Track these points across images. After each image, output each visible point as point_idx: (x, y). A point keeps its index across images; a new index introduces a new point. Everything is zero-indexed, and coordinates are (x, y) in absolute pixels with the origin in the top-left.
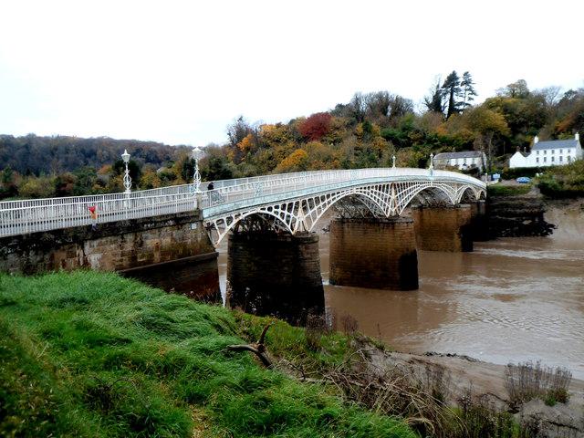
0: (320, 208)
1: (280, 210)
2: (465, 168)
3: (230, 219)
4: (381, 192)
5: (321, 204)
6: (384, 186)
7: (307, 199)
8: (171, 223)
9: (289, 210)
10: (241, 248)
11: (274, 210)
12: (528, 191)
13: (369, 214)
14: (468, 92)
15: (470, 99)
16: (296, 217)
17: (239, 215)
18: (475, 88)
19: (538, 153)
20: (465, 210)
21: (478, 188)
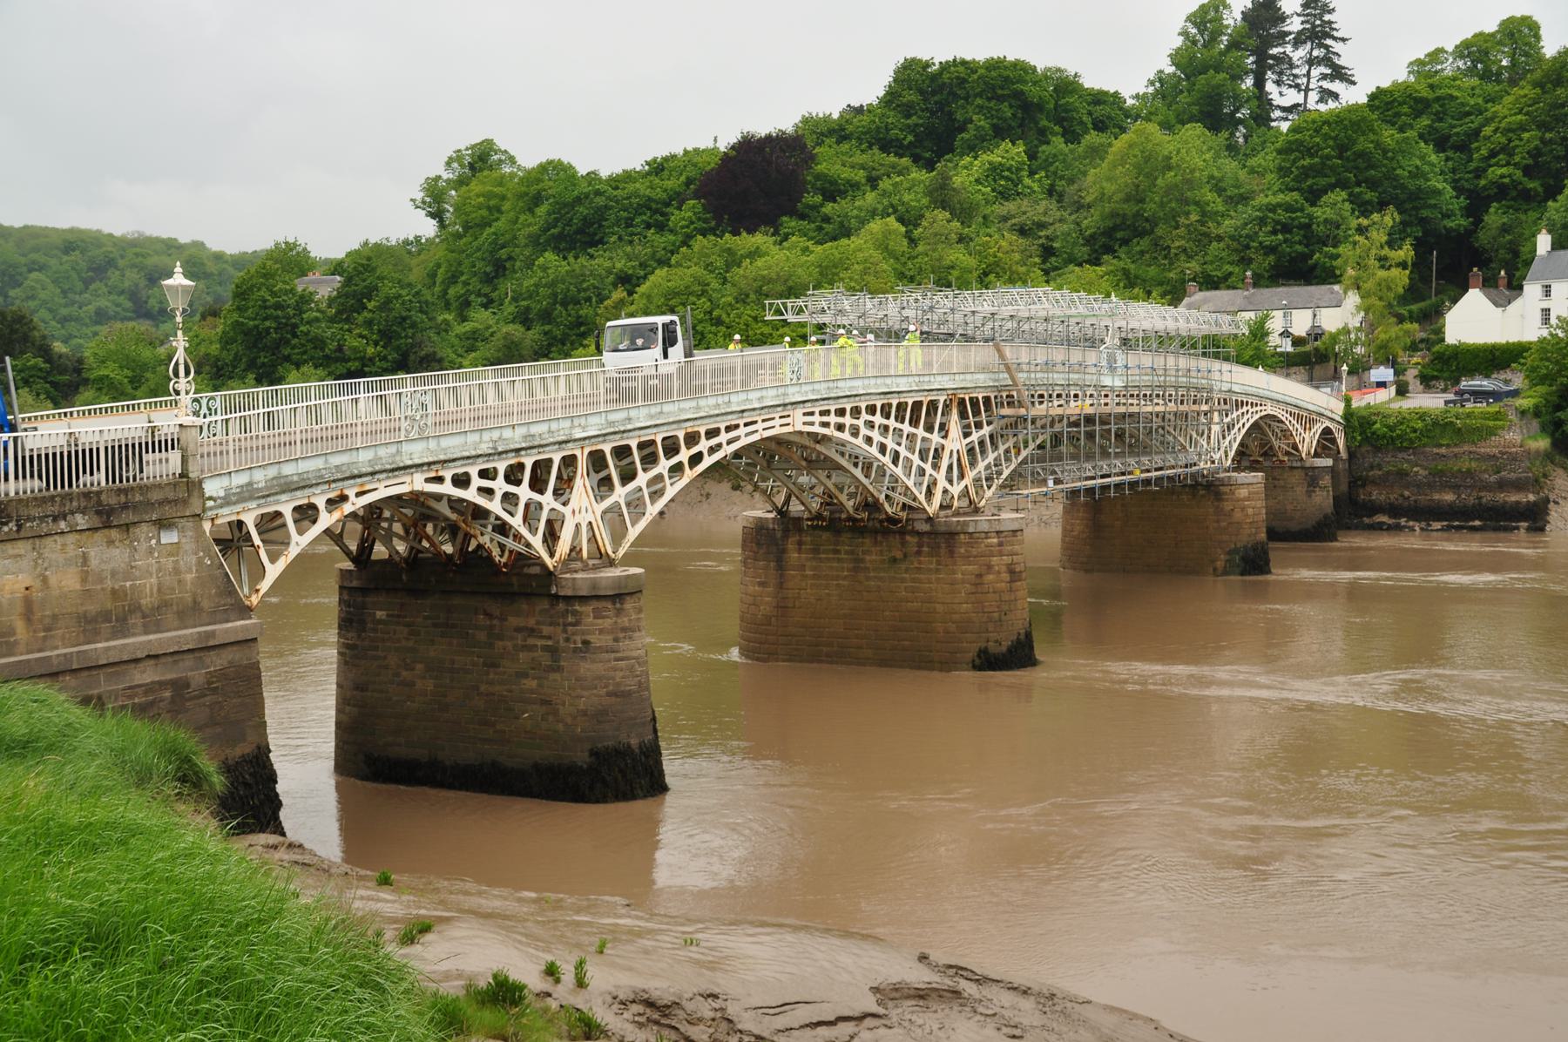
0: (659, 478)
1: (500, 486)
2: (1287, 347)
3: (306, 514)
4: (906, 428)
5: (664, 465)
6: (917, 405)
7: (607, 448)
8: (81, 521)
9: (538, 485)
10: (380, 614)
11: (477, 482)
12: (1492, 432)
13: (872, 506)
14: (1316, 72)
15: (1327, 95)
16: (566, 511)
17: (343, 498)
18: (1346, 56)
19: (1547, 291)
20: (1243, 492)
21: (1307, 418)
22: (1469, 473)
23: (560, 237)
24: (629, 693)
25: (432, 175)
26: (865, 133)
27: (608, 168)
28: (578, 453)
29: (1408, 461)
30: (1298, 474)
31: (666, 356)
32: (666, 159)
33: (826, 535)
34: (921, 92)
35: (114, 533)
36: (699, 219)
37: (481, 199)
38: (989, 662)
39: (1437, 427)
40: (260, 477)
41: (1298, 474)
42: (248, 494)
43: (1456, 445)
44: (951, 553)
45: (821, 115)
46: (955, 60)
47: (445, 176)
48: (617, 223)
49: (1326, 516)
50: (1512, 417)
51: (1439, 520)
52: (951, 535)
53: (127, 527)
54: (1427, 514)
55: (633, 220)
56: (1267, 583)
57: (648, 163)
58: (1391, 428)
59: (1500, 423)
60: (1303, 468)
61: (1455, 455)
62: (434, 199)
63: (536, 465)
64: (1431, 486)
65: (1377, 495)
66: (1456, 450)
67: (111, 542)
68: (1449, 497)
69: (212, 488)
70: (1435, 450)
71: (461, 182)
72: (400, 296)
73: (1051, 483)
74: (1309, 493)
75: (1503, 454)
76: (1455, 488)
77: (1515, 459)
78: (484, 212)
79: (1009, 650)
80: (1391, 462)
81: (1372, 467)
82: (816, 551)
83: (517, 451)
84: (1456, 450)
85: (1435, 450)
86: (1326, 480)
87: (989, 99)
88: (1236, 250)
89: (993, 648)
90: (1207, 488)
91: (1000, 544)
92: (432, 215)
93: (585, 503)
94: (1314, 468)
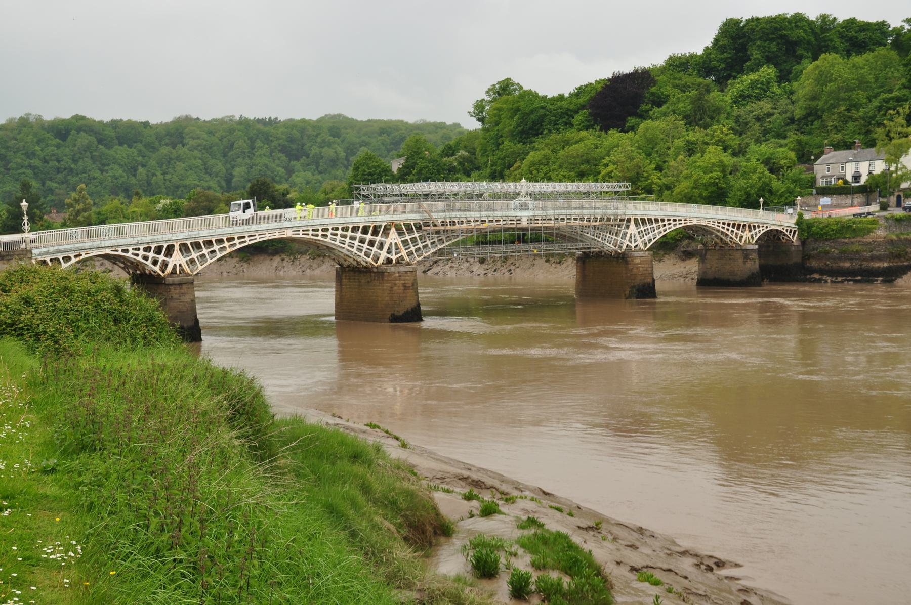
7: (188, 243)
11: (131, 251)
12: (870, 231)
20: (638, 261)
22: (857, 252)
23: (522, 132)
24: (183, 312)
25: (480, 99)
26: (696, 65)
27: (551, 93)
28: (175, 244)
29: (830, 246)
30: (740, 253)
31: (244, 212)
32: (586, 86)
33: (352, 273)
34: (732, 38)
35: (5, 261)
36: (586, 120)
37: (495, 112)
38: (395, 319)
39: (845, 228)
40: (51, 249)
41: (740, 253)
42: (47, 253)
43: (854, 238)
44: (383, 280)
45: (680, 55)
46: (752, 18)
47: (487, 98)
48: (550, 123)
49: (753, 274)
50: (882, 222)
51: (842, 276)
52: (383, 273)
53: (9, 260)
54: (837, 273)
55: (558, 121)
56: (655, 303)
57: (576, 89)
58: (822, 229)
59: (874, 226)
60: (741, 250)
61: (852, 243)
62: (479, 111)
63: (168, 246)
64: (840, 259)
65: (814, 264)
66: (853, 240)
67: (4, 263)
68: (847, 264)
69: (34, 251)
70: (843, 240)
71: (494, 100)
72: (428, 167)
73: (455, 255)
74: (744, 262)
75: (874, 242)
76: (851, 259)
77: (879, 245)
78: (496, 119)
79: (403, 315)
80: (823, 246)
81: (814, 249)
82: (349, 279)
83: (148, 243)
84: (853, 240)
85: (843, 240)
86: (754, 256)
87: (765, 41)
88: (865, 126)
89: (396, 314)
90: (622, 258)
91: (400, 276)
92: (479, 120)
93: (178, 258)
94: (747, 250)
